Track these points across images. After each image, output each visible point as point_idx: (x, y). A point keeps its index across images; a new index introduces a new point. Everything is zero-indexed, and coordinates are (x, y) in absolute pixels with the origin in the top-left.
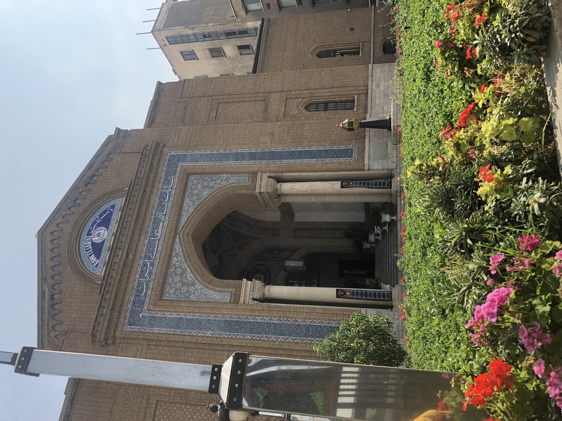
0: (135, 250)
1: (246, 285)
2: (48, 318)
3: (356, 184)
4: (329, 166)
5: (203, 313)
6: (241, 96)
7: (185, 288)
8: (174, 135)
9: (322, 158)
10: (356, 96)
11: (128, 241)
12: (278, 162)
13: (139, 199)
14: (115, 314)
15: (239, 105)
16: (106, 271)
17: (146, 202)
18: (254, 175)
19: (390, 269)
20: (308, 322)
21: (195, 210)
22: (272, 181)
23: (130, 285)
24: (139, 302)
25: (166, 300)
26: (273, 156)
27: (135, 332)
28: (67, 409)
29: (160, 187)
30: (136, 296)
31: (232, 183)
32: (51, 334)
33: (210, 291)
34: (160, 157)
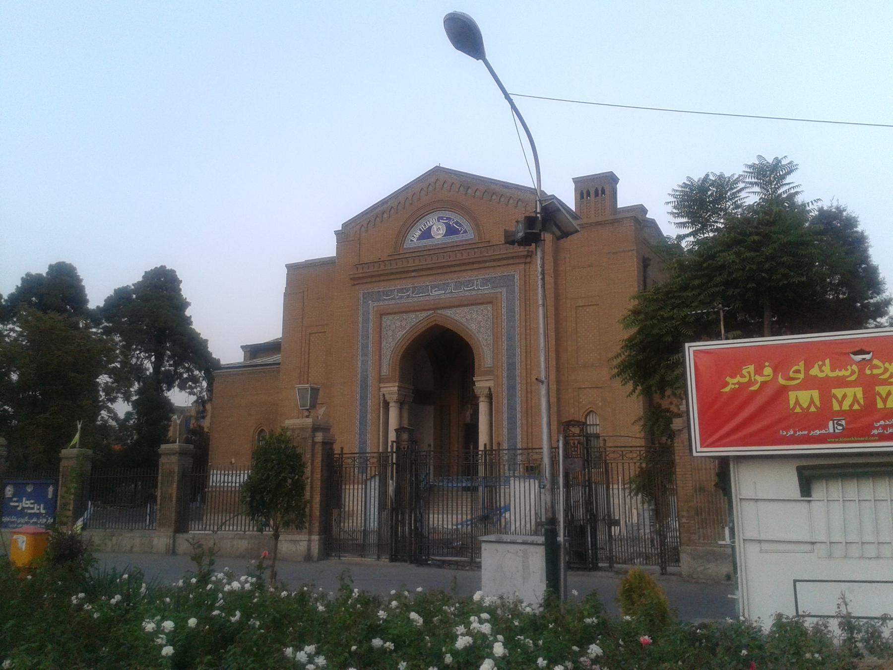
1: (394, 386)
7: (390, 333)
17: (463, 268)
18: (490, 372)
22: (486, 391)
30: (383, 292)
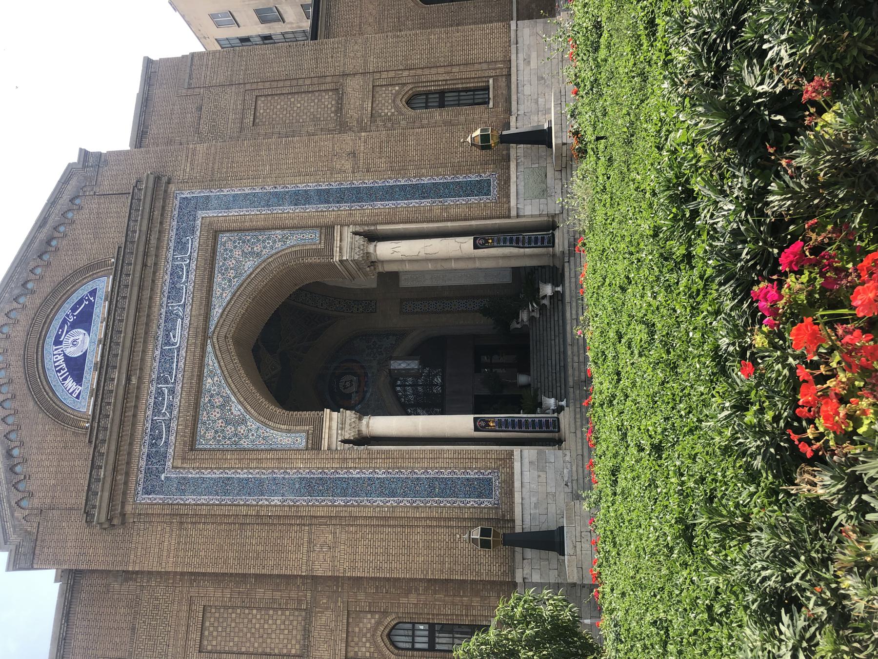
0: (141, 369)
1: (331, 419)
2: (8, 489)
3: (499, 241)
4: (453, 211)
5: (264, 469)
6: (294, 83)
7: (230, 429)
8: (183, 161)
9: (441, 197)
10: (491, 81)
11: (126, 353)
12: (367, 206)
13: (137, 280)
14: (120, 478)
15: (292, 100)
16: (95, 405)
18: (328, 230)
19: (554, 368)
20: (432, 474)
21: (234, 295)
23: (139, 428)
24: (157, 456)
25: (201, 450)
26: (358, 195)
27: (156, 504)
28: (61, 629)
29: (170, 255)
30: (152, 445)
31: (293, 246)
32: (16, 514)
33: (272, 431)
34: (164, 201)
